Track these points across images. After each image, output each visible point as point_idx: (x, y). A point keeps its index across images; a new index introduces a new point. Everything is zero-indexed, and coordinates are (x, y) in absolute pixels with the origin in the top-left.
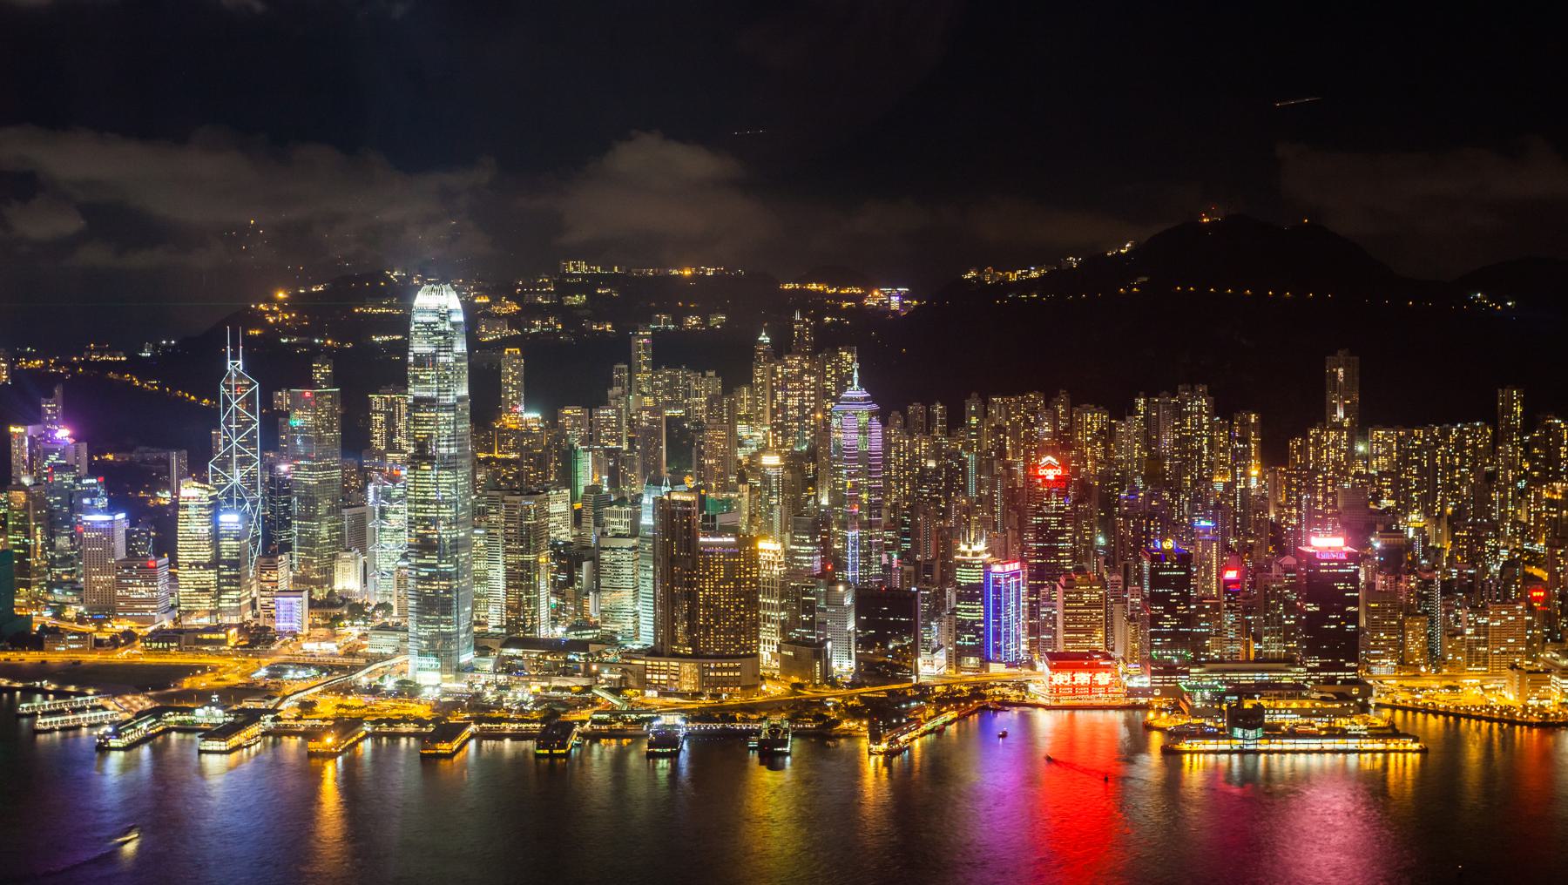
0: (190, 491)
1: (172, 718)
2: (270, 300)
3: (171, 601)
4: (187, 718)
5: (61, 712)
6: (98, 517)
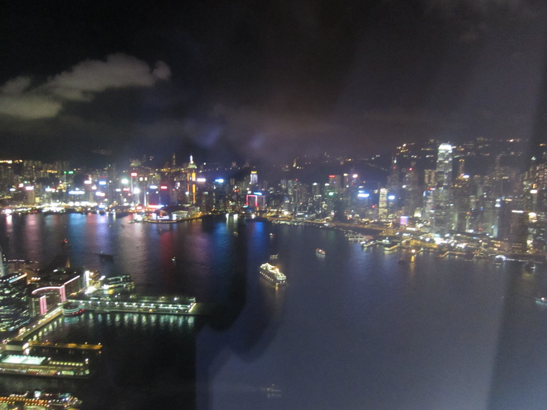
0: (383, 191)
1: (378, 241)
2: (402, 147)
3: (377, 215)
4: (381, 242)
5: (353, 237)
6: (362, 195)
